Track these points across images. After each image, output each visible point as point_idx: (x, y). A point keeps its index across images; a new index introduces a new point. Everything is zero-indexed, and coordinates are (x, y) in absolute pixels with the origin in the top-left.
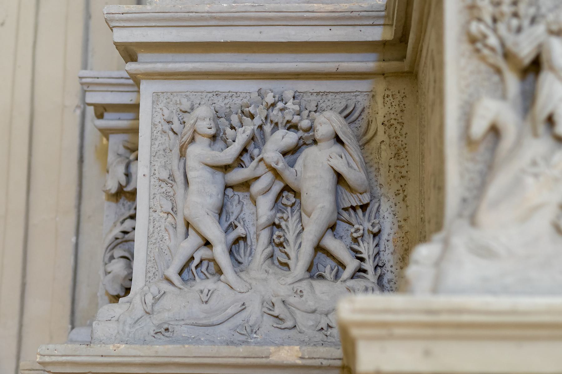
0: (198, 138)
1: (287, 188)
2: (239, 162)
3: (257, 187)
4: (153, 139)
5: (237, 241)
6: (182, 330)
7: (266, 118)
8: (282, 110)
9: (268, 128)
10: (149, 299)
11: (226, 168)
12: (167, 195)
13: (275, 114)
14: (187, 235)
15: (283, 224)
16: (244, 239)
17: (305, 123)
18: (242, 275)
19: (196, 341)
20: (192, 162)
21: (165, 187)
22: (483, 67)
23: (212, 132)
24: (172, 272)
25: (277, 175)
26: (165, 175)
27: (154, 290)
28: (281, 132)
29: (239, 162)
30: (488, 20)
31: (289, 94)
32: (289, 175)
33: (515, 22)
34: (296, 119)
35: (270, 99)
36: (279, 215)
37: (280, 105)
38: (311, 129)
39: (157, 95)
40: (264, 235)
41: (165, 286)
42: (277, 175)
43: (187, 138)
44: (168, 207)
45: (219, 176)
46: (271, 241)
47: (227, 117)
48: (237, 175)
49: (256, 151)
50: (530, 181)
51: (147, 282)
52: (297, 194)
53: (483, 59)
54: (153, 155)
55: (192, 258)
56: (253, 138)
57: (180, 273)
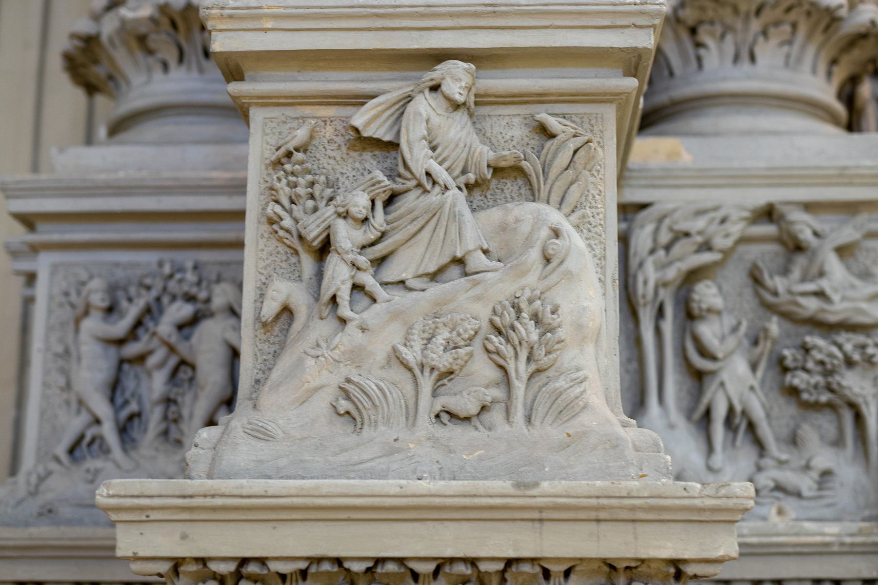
1: (183, 363)
3: (152, 361)
4: (50, 312)
5: (131, 417)
6: (66, 511)
7: (165, 289)
8: (181, 281)
9: (165, 300)
10: (34, 479)
11: (120, 342)
13: (172, 285)
14: (79, 412)
15: (180, 399)
17: (203, 295)
18: (133, 454)
19: (80, 522)
20: (84, 336)
21: (61, 362)
22: (281, 248)
23: (106, 304)
24: (61, 450)
25: (172, 349)
26: (60, 349)
27: (41, 469)
28: (178, 304)
30: (285, 202)
31: (189, 265)
32: (183, 349)
33: (310, 203)
34: (194, 290)
35: (167, 269)
36: (175, 390)
37: (178, 276)
38: (208, 301)
39: (54, 269)
41: (53, 466)
42: (172, 349)
43: (80, 309)
44: (62, 381)
45: (112, 351)
46: (165, 418)
47: (125, 289)
48: (132, 349)
51: (39, 459)
52: (193, 367)
53: (280, 240)
54: (50, 329)
56: (148, 310)
57: (71, 451)
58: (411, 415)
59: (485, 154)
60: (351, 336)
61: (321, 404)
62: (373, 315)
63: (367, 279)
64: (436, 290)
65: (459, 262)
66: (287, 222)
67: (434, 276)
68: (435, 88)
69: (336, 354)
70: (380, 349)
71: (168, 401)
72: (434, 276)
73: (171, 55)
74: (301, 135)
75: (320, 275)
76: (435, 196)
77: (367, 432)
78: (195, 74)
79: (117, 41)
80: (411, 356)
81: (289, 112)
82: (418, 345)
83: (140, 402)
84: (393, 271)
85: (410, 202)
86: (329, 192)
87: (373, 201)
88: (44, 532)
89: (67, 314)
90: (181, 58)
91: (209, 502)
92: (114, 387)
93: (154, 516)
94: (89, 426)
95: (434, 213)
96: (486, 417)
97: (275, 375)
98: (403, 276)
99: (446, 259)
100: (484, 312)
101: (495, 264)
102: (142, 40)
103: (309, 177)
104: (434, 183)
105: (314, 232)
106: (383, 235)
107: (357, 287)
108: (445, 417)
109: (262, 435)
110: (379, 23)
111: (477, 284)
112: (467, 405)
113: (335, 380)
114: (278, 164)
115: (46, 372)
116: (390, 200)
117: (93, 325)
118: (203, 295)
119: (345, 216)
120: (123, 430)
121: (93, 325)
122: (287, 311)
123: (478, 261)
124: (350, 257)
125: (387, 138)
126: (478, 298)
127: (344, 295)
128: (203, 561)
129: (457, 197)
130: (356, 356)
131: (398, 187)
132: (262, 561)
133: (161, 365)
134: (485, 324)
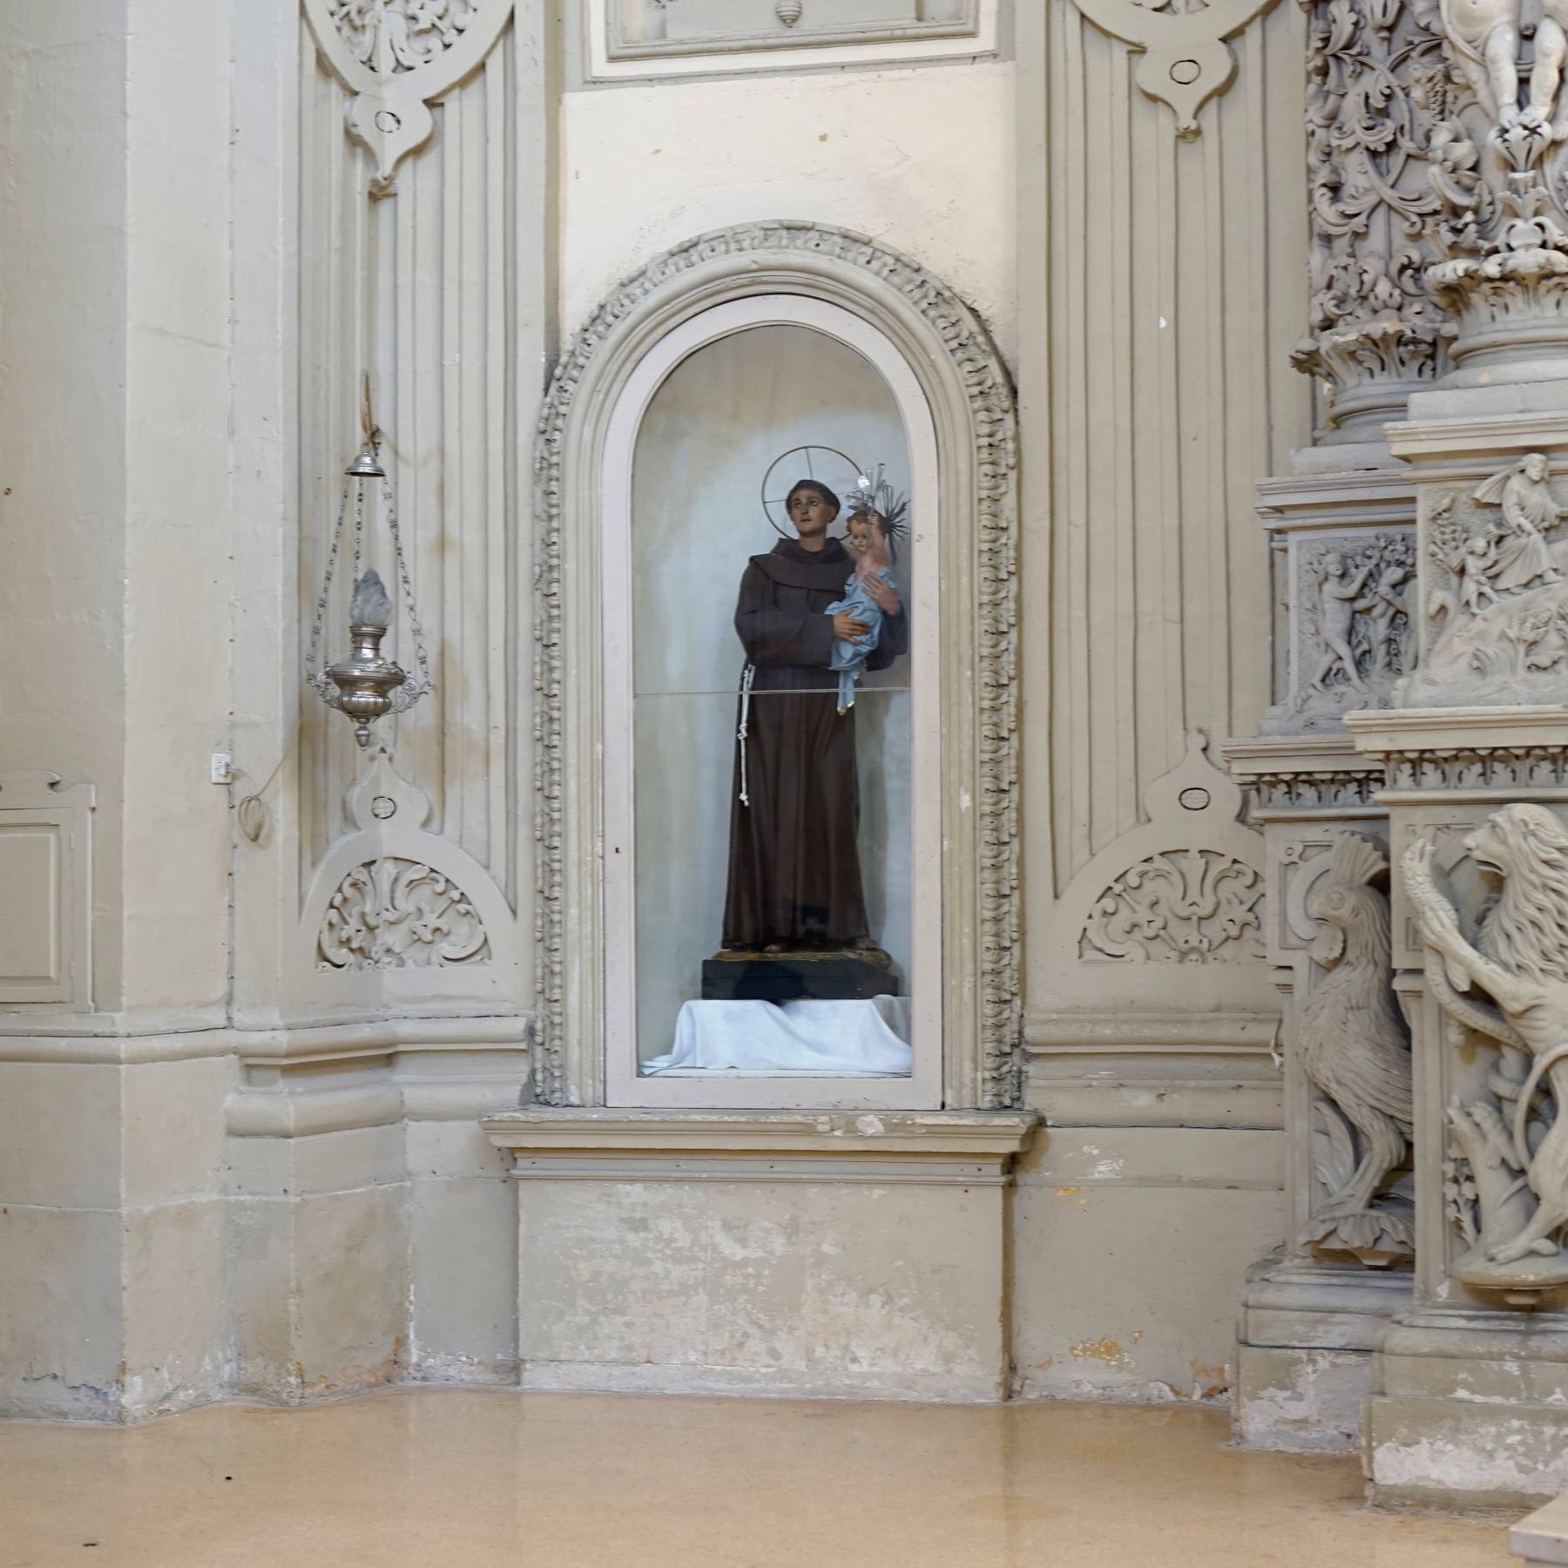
0: (1331, 578)
1: (1398, 611)
2: (1360, 594)
3: (1376, 612)
4: (1299, 578)
5: (1364, 653)
6: (1323, 723)
7: (1381, 557)
9: (1383, 565)
10: (1299, 702)
11: (1352, 600)
12: (1312, 621)
13: (1387, 554)
14: (1326, 651)
16: (1369, 651)
17: (1409, 561)
18: (1366, 680)
21: (1311, 615)
23: (1339, 573)
24: (1316, 680)
25: (1390, 603)
26: (1309, 605)
27: (1303, 694)
28: (1393, 568)
29: (1360, 594)
30: (1439, 543)
31: (1399, 537)
32: (1398, 602)
33: (1454, 544)
34: (1403, 558)
35: (1382, 543)
39: (1300, 544)
40: (1383, 649)
41: (1312, 691)
42: (1390, 603)
43: (1322, 577)
44: (1313, 630)
45: (1347, 605)
46: (1388, 653)
47: (1352, 558)
48: (1361, 604)
49: (1373, 585)
50: (1456, 640)
51: (1301, 687)
52: (1406, 615)
54: (1300, 590)
55: (1330, 669)
56: (1371, 575)
57: (1323, 680)
58: (1513, 667)
59: (1554, 509)
60: (1478, 625)
61: (1463, 663)
62: (1490, 611)
63: (1487, 590)
64: (1527, 594)
65: (1540, 576)
66: (1441, 556)
67: (1526, 585)
68: (1522, 471)
69: (1470, 634)
70: (1494, 630)
71: (1390, 641)
72: (1526, 585)
73: (1376, 366)
74: (1446, 502)
75: (1461, 585)
76: (1523, 540)
77: (1489, 679)
78: (1396, 379)
79: (1332, 354)
80: (1512, 634)
81: (1439, 485)
82: (1516, 628)
83: (1369, 643)
84: (1502, 583)
85: (1508, 542)
86: (1464, 536)
87: (1489, 543)
88: (1309, 738)
89: (1312, 579)
90: (1383, 369)
91: (1401, 721)
92: (1351, 631)
93: (1374, 729)
94: (1334, 662)
95: (1523, 549)
96: (1557, 667)
97: (1438, 647)
98: (1509, 586)
99: (1530, 576)
100: (1554, 606)
101: (1560, 578)
102: (1352, 354)
103: (1452, 528)
104: (1523, 531)
105: (1455, 563)
106: (1496, 563)
107: (1481, 594)
108: (1533, 668)
109: (1431, 682)
110: (1488, 432)
111: (1549, 590)
112: (1544, 660)
113: (1470, 649)
114: (1434, 519)
115: (1301, 623)
116: (1500, 539)
117: (1331, 587)
118: (1409, 561)
119: (1472, 553)
120: (1359, 664)
121: (1331, 587)
122: (1443, 609)
123: (1551, 576)
124: (1476, 578)
125: (1497, 502)
126: (1550, 599)
127: (1474, 600)
128: (1401, 752)
129: (1537, 537)
130: (1482, 635)
131: (1503, 533)
132: (1432, 751)
133: (1383, 615)
134: (1555, 615)
